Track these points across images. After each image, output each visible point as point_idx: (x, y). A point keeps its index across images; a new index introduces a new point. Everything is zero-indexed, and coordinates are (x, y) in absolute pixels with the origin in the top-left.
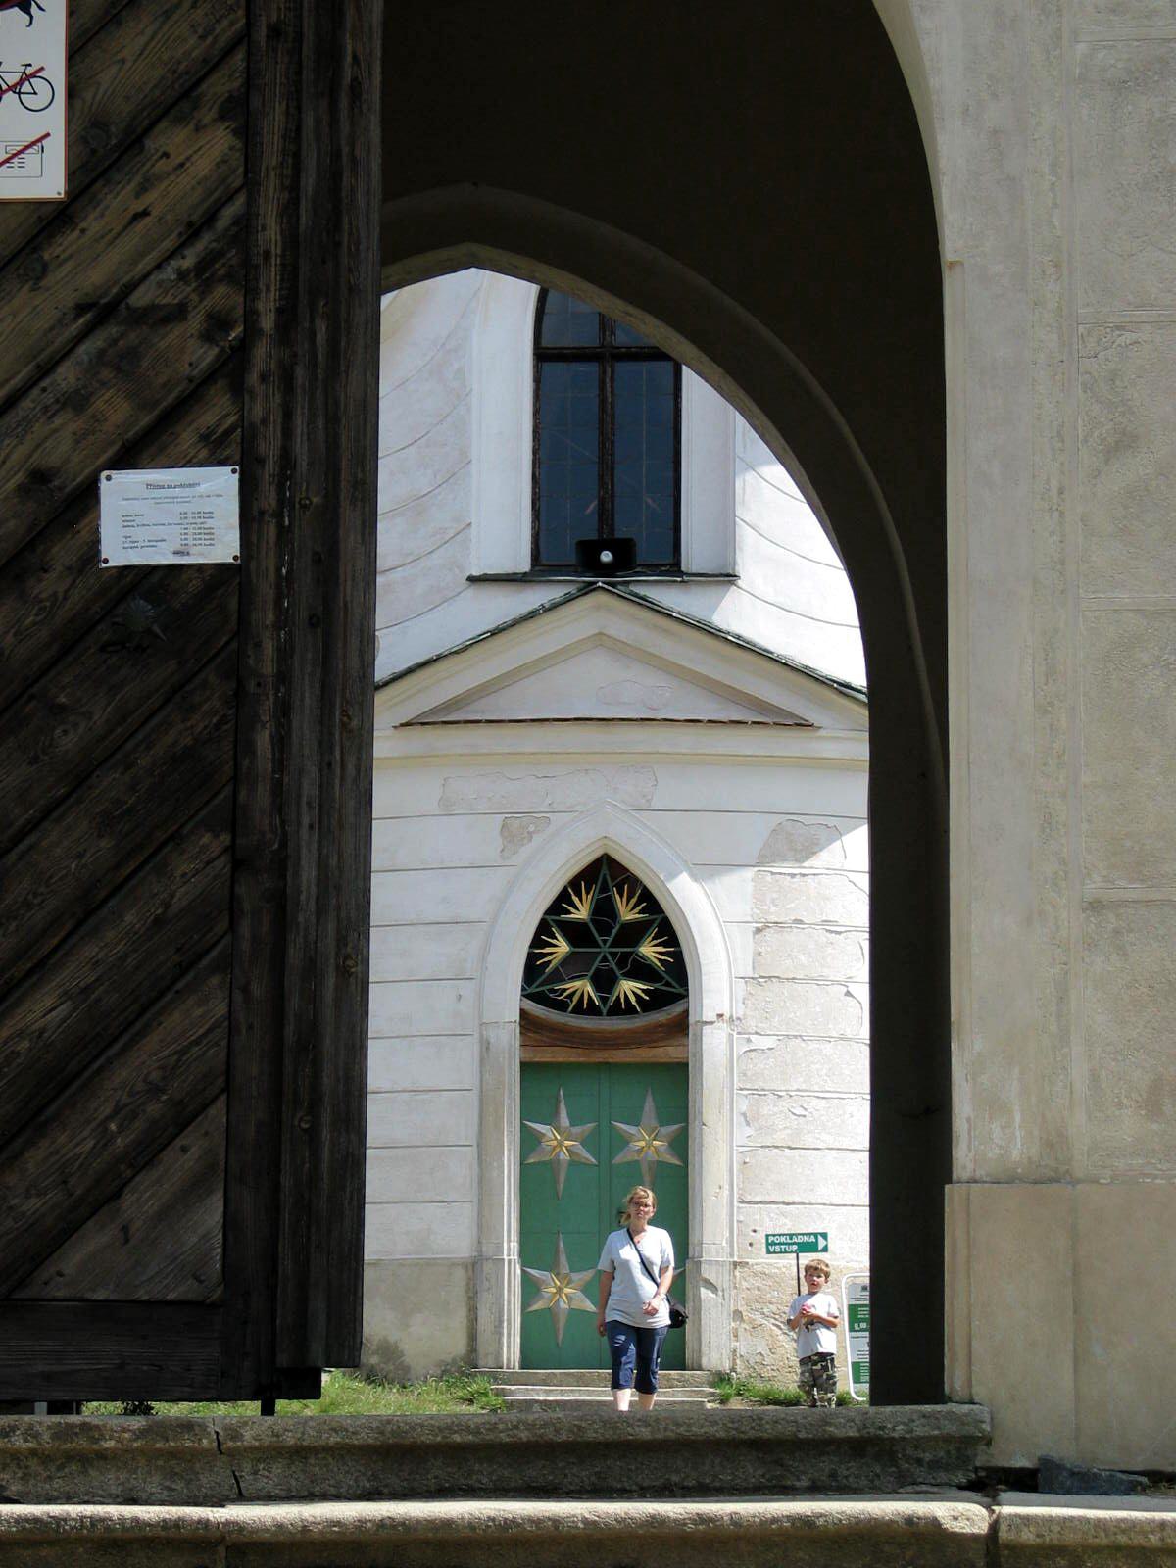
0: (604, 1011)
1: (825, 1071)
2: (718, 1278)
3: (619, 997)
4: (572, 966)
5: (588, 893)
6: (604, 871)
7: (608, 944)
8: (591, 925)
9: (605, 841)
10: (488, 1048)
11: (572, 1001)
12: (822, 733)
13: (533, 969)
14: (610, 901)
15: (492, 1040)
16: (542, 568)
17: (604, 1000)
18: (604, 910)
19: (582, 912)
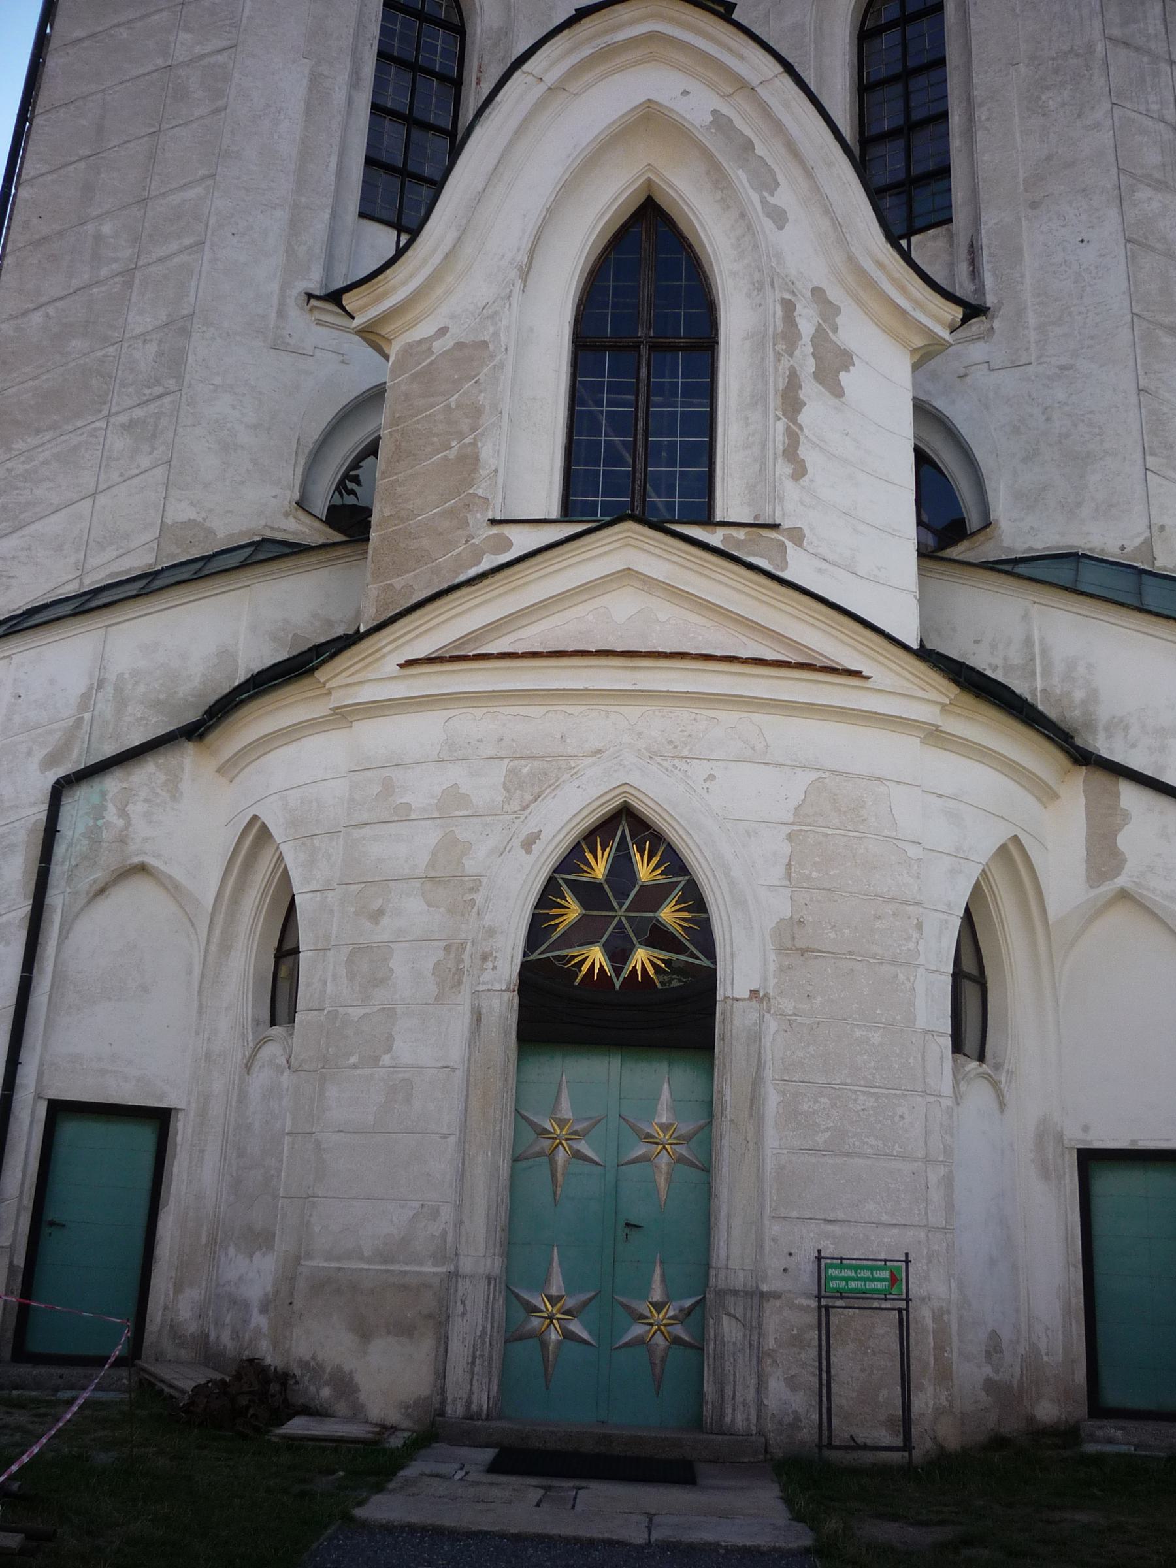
0: (617, 985)
1: (873, 1064)
2: (745, 1314)
3: (635, 967)
4: (583, 933)
5: (603, 850)
6: (624, 828)
7: (625, 907)
8: (606, 886)
9: (626, 788)
10: (479, 1020)
11: (580, 971)
12: (869, 684)
13: (538, 929)
14: (629, 858)
15: (484, 1011)
16: (568, 512)
17: (618, 971)
18: (622, 868)
19: (600, 869)
